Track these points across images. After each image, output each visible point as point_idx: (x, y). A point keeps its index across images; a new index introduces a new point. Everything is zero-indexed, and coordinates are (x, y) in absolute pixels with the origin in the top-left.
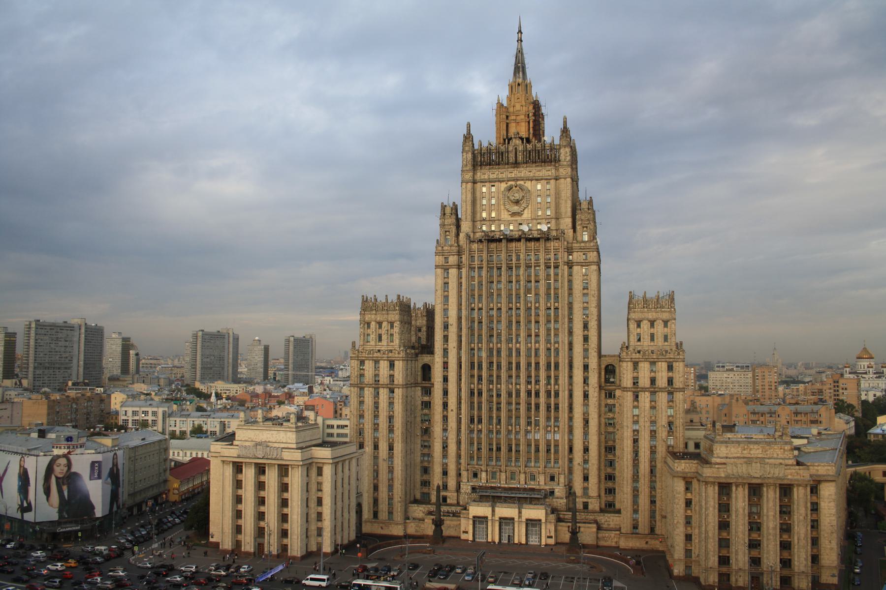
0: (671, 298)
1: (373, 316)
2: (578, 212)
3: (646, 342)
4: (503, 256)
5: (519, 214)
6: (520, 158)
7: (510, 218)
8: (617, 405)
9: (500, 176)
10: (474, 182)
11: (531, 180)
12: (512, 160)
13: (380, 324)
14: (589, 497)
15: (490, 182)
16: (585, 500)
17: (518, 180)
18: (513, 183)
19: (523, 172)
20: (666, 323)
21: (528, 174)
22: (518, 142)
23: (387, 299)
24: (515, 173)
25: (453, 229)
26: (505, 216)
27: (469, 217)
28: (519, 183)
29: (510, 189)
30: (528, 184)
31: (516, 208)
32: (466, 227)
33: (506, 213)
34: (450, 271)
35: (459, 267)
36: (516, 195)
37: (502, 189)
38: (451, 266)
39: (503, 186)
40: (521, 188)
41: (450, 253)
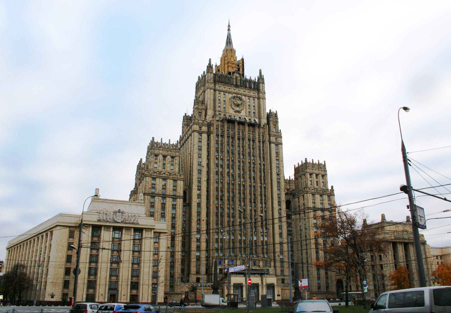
3: (315, 186)
4: (237, 131)
5: (239, 112)
8: (293, 223)
9: (228, 90)
10: (215, 90)
11: (245, 96)
12: (235, 83)
13: (165, 157)
14: (285, 276)
15: (224, 92)
16: (283, 277)
18: (236, 95)
19: (242, 91)
20: (323, 176)
21: (243, 93)
23: (170, 142)
24: (237, 90)
25: (204, 112)
26: (231, 112)
27: (212, 108)
28: (239, 96)
29: (234, 98)
30: (243, 97)
31: (237, 109)
32: (210, 113)
34: (203, 135)
35: (209, 134)
36: (238, 101)
37: (230, 97)
38: (203, 132)
39: (230, 95)
40: (240, 99)
41: (203, 125)
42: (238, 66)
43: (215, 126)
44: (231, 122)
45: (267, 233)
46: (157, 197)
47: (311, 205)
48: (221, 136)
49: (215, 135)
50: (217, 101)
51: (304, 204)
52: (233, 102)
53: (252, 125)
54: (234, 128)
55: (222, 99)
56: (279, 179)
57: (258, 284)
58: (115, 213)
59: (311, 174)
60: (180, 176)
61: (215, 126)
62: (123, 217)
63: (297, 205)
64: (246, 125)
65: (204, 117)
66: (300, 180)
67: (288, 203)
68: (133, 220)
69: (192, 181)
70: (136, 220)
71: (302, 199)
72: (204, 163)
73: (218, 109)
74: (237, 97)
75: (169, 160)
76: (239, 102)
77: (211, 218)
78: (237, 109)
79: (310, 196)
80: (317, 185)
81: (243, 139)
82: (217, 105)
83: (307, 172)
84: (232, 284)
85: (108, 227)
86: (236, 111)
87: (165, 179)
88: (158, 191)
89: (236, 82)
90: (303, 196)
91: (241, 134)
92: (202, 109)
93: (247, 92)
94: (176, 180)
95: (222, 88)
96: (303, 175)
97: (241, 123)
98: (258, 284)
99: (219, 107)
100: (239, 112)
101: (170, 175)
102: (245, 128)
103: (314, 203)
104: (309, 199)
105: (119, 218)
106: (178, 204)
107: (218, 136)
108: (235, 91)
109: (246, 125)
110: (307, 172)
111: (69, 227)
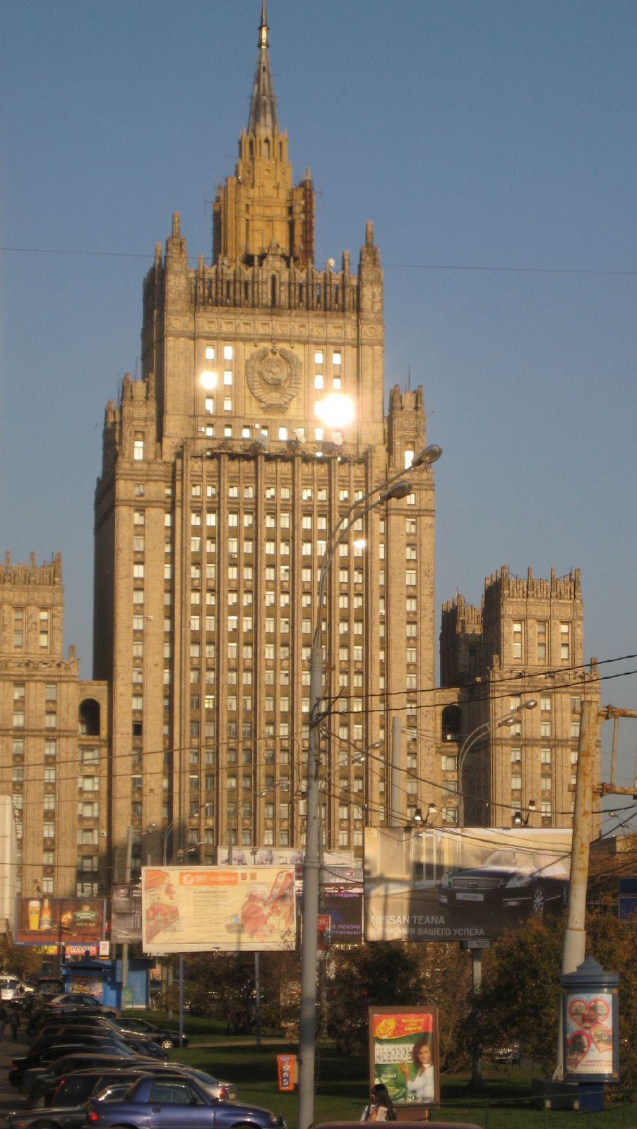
0: (575, 583)
2: (398, 412)
6: (283, 297)
7: (261, 415)
12: (267, 298)
17: (279, 340)
18: (268, 346)
22: (279, 264)
28: (280, 346)
29: (263, 356)
30: (299, 351)
31: (273, 397)
33: (255, 403)
36: (276, 370)
37: (248, 357)
40: (287, 359)
52: (260, 374)
86: (270, 406)
92: (145, 420)
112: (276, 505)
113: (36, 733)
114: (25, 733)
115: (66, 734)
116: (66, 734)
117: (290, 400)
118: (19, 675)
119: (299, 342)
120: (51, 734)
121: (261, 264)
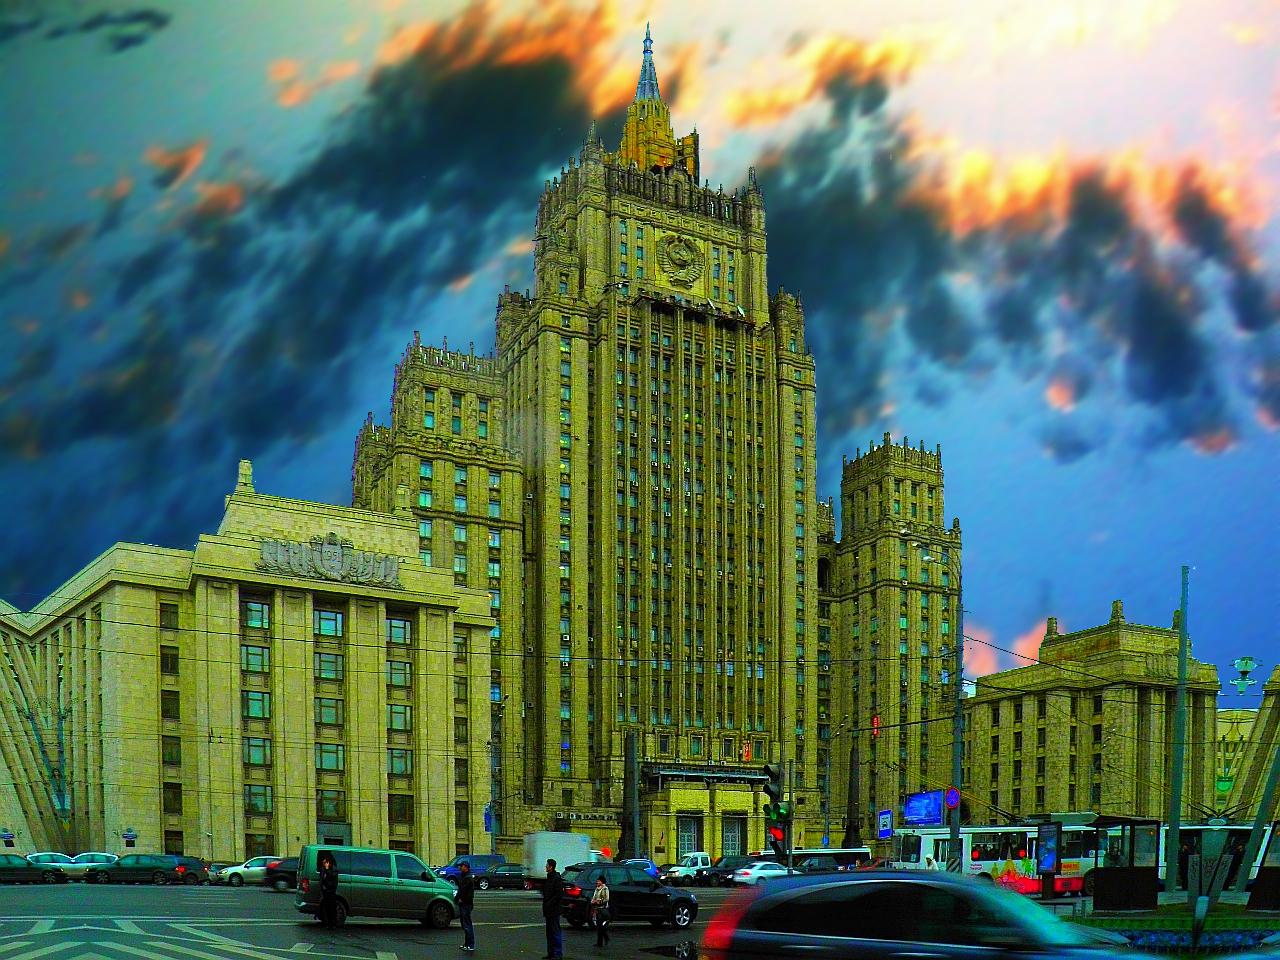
1: (444, 377)
3: (909, 516)
4: (681, 337)
5: (686, 285)
10: (609, 215)
11: (705, 240)
19: (693, 223)
24: (679, 220)
30: (700, 243)
31: (682, 274)
39: (659, 234)
40: (690, 247)
42: (680, 153)
43: (614, 319)
44: (664, 308)
45: (763, 654)
46: (440, 521)
47: (897, 574)
48: (632, 348)
49: (614, 343)
50: (618, 249)
51: (874, 570)
53: (728, 324)
54: (674, 329)
55: (632, 240)
56: (802, 493)
57: (746, 813)
58: (316, 543)
59: (898, 482)
60: (511, 458)
61: (614, 316)
62: (348, 561)
63: (851, 573)
64: (711, 323)
65: (577, 290)
66: (860, 497)
67: (824, 565)
68: (381, 573)
69: (544, 483)
70: (394, 574)
71: (869, 555)
72: (580, 429)
73: (618, 269)
74: (680, 241)
75: (473, 406)
76: (686, 255)
77: (604, 601)
78: (682, 274)
79: (894, 544)
80: (914, 515)
81: (699, 365)
82: (618, 258)
83: (888, 475)
84: (673, 809)
85: (295, 594)
87: (462, 466)
88: (441, 502)
89: (676, 198)
90: (874, 546)
91: (694, 347)
93: (710, 228)
94: (499, 472)
95: (632, 208)
96: (873, 482)
97: (697, 316)
98: (746, 813)
99: (624, 264)
100: (686, 285)
101: (478, 453)
102: (706, 330)
103: (904, 567)
104: (892, 553)
105: (333, 566)
106: (509, 548)
107: (622, 347)
108: (675, 224)
109: (711, 323)
110: (888, 475)
111: (158, 590)
112: (691, 356)
113: (481, 521)
114: (468, 519)
115: (511, 525)
116: (511, 525)
117: (694, 280)
118: (461, 458)
119: (701, 238)
120: (495, 524)
121: (667, 174)
